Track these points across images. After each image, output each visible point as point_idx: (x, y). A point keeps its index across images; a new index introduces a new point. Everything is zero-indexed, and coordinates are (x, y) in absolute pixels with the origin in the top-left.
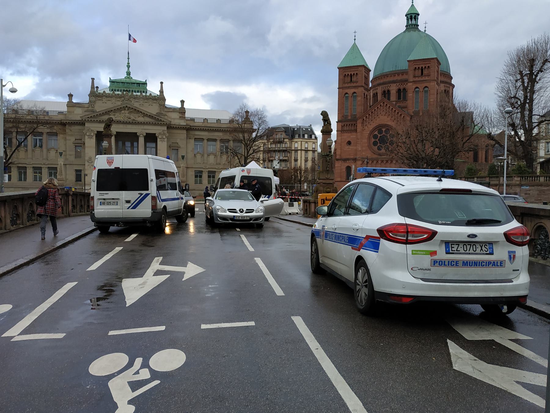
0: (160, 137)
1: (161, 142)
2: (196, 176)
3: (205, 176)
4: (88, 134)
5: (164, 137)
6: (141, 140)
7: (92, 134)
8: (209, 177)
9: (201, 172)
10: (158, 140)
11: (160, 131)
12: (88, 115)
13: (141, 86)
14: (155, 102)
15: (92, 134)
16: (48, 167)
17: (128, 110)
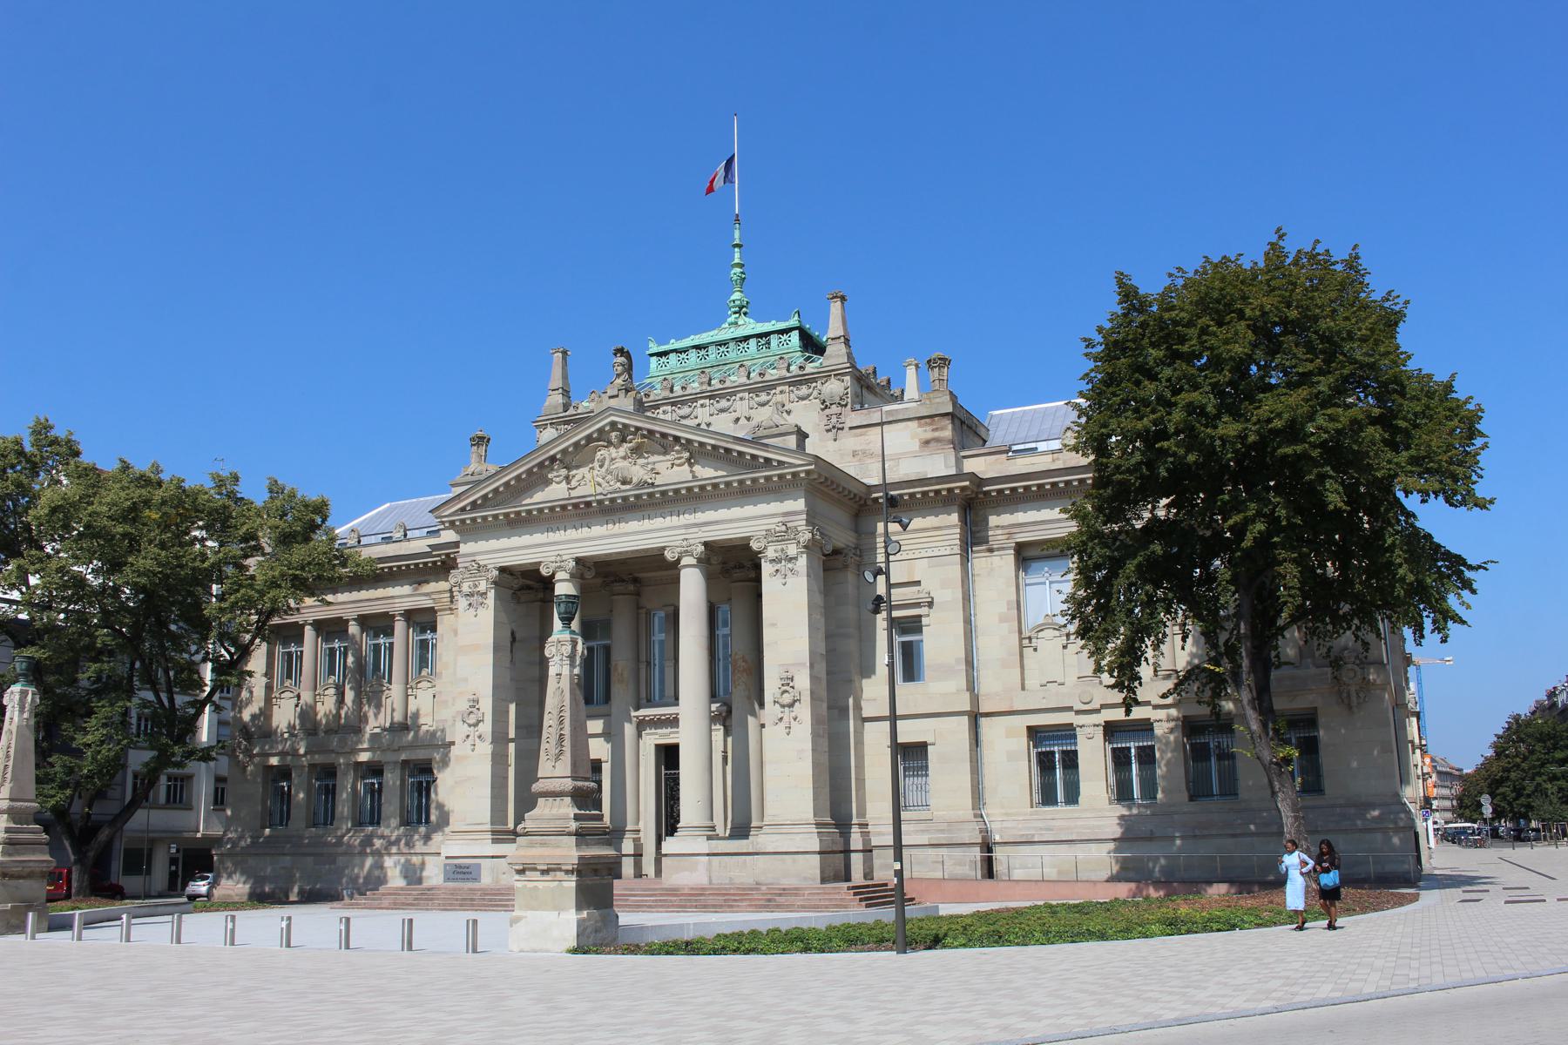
0: (771, 553)
1: (779, 579)
2: (1045, 763)
3: (1093, 756)
4: (466, 588)
5: (792, 550)
6: (692, 589)
7: (483, 586)
8: (1120, 760)
9: (1067, 732)
10: (767, 569)
11: (773, 524)
12: (458, 497)
13: (774, 339)
14: (804, 390)
15: (483, 586)
16: (405, 763)
17: (623, 440)
